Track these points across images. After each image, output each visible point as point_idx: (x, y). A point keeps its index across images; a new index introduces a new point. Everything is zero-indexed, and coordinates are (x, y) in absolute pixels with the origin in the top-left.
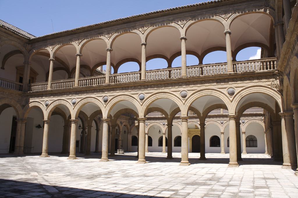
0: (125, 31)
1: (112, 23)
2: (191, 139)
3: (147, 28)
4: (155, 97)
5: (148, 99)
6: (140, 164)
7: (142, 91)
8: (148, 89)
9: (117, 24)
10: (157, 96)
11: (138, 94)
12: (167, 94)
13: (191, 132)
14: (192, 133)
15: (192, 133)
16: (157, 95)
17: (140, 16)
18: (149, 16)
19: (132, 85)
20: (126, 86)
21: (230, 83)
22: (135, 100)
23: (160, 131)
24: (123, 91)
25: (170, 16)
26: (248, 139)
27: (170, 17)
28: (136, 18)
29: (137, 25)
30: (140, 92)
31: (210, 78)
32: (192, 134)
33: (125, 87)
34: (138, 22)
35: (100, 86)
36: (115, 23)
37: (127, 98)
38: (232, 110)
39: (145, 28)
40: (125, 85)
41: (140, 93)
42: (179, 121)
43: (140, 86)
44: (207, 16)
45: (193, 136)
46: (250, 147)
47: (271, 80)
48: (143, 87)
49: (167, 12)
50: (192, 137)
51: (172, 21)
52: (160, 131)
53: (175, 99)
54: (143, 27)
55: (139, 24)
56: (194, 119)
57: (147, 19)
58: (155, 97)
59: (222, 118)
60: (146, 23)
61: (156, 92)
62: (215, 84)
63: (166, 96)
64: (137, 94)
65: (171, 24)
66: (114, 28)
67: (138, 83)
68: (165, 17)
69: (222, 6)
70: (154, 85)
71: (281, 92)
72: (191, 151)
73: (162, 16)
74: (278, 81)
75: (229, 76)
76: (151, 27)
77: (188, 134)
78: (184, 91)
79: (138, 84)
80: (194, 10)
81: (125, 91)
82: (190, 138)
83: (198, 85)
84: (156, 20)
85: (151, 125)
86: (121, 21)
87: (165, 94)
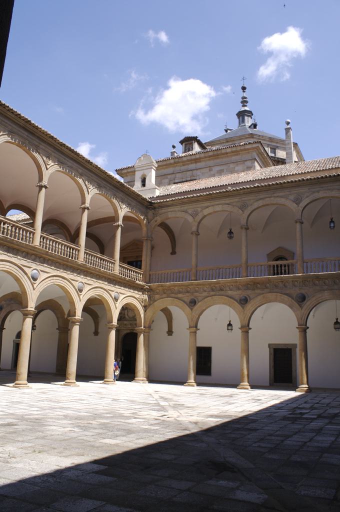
0: (23, 143)
1: (9, 113)
3: (53, 164)
4: (52, 281)
5: (44, 282)
6: (27, 389)
7: (37, 264)
8: (44, 265)
9: (14, 122)
10: (54, 281)
11: (31, 269)
12: (65, 281)
16: (54, 278)
17: (52, 138)
18: (61, 147)
19: (24, 249)
20: (16, 247)
21: (116, 286)
22: (25, 277)
24: (9, 254)
25: (80, 167)
27: (80, 168)
28: (46, 137)
29: (41, 146)
30: (34, 266)
31: (86, 268)
33: (14, 249)
34: (43, 144)
35: (12, 242)
36: (13, 116)
37: (14, 270)
38: (32, 306)
39: (51, 161)
40: (18, 245)
41: (34, 268)
43: (36, 255)
44: (109, 193)
47: (139, 293)
48: (38, 260)
49: (80, 159)
51: (81, 175)
53: (72, 291)
54: (49, 159)
55: (43, 148)
57: (55, 148)
58: (52, 281)
60: (53, 154)
61: (55, 274)
62: (106, 283)
63: (64, 283)
64: (30, 268)
65: (78, 179)
66: (6, 123)
67: (36, 250)
68: (75, 164)
69: (122, 191)
70: (52, 261)
71: (145, 307)
73: (71, 159)
74: (146, 296)
75: (120, 279)
76: (57, 166)
78: (82, 282)
79: (37, 252)
80: (101, 178)
81: (11, 255)
83: (94, 280)
84: (65, 159)
86: (23, 122)
87: (63, 280)
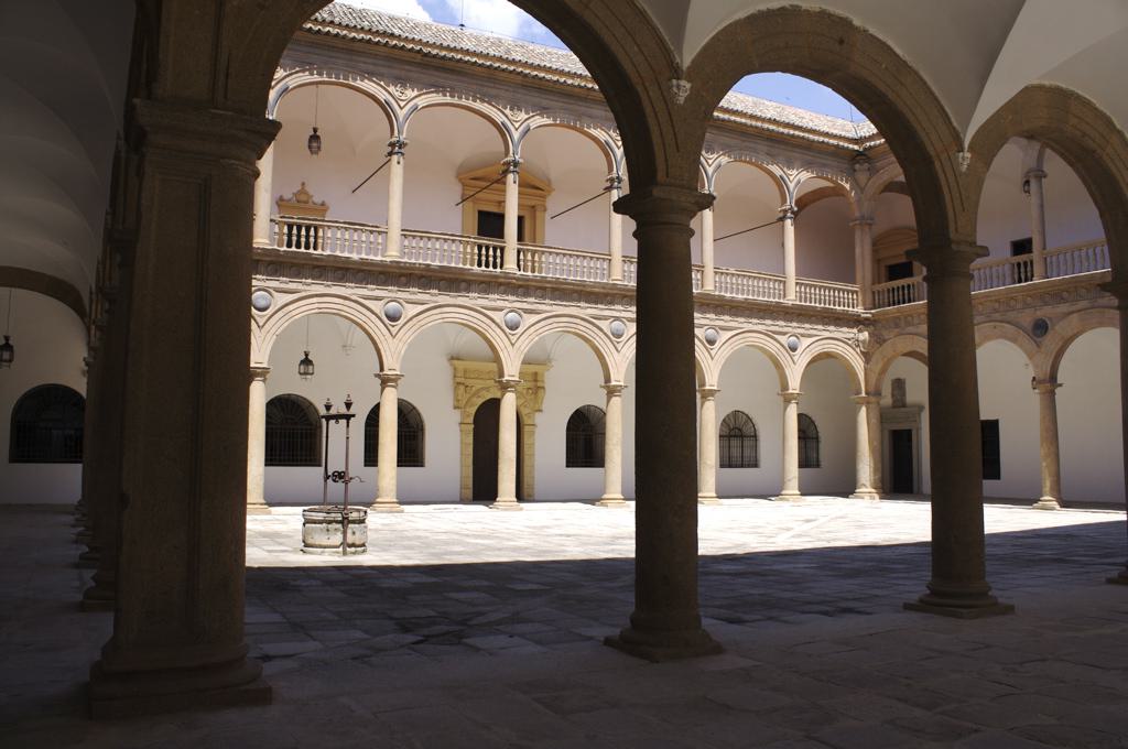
2: (471, 420)
13: (468, 382)
14: (478, 384)
15: (478, 384)
23: (307, 362)
26: (726, 431)
32: (477, 394)
42: (493, 304)
45: (480, 401)
46: (730, 466)
50: (473, 410)
52: (307, 362)
56: (582, 304)
59: (712, 316)
72: (469, 493)
77: (455, 389)
82: (464, 415)
85: (301, 310)
